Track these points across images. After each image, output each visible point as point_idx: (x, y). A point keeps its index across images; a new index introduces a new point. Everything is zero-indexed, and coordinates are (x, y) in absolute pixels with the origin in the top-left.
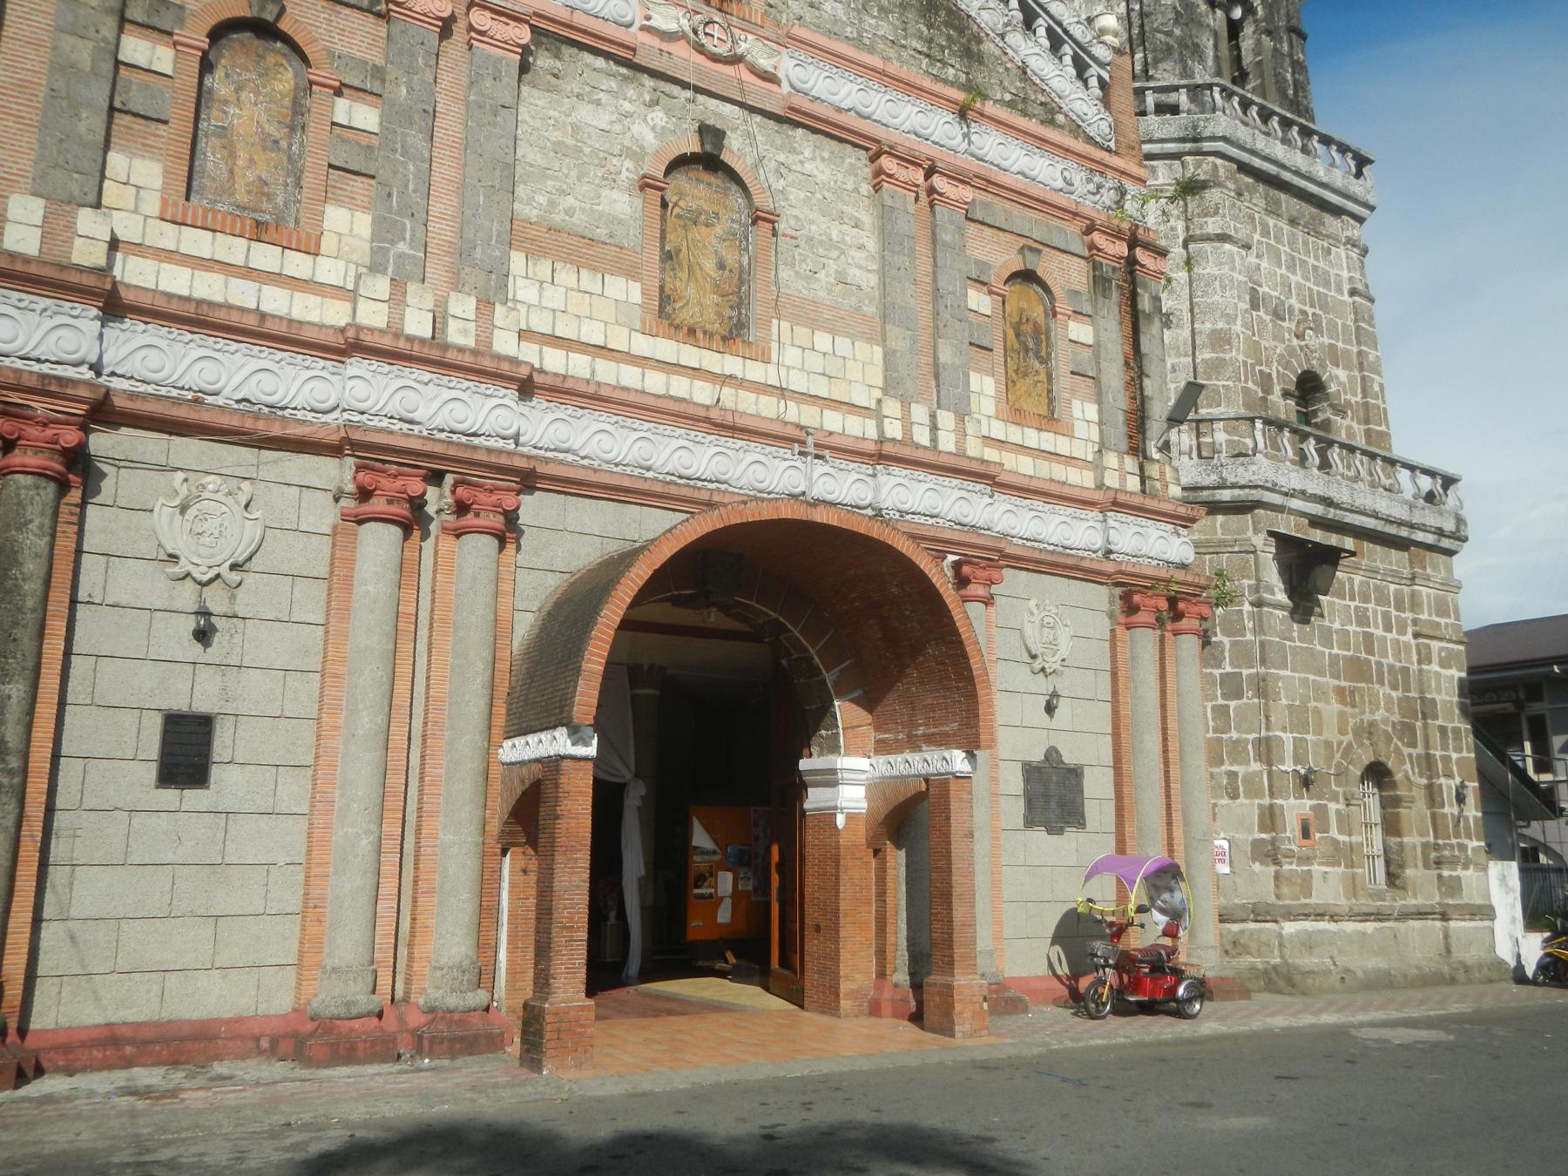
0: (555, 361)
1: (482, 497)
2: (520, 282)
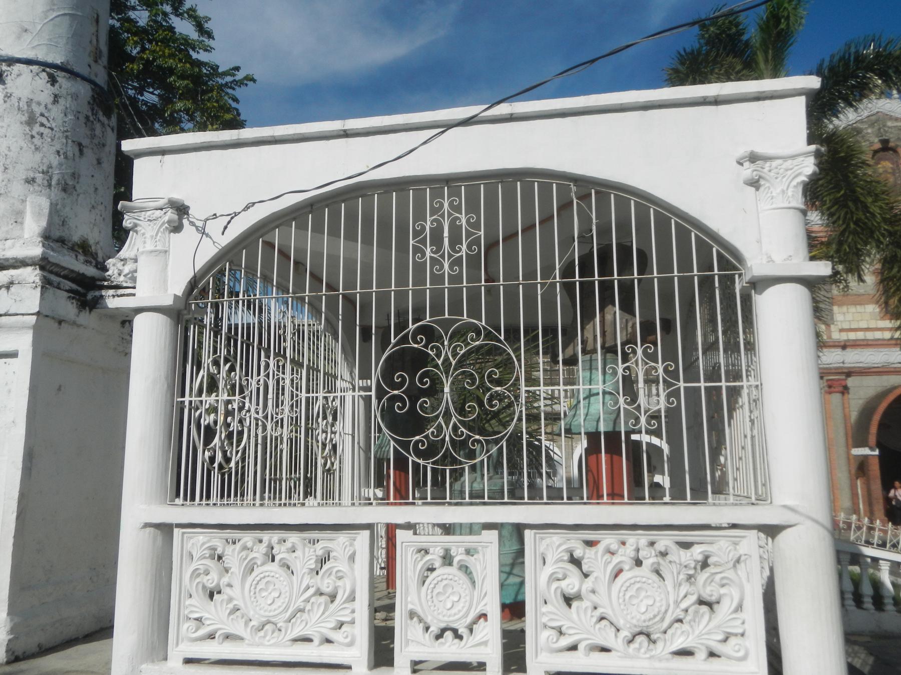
0: (852, 336)
2: (837, 315)
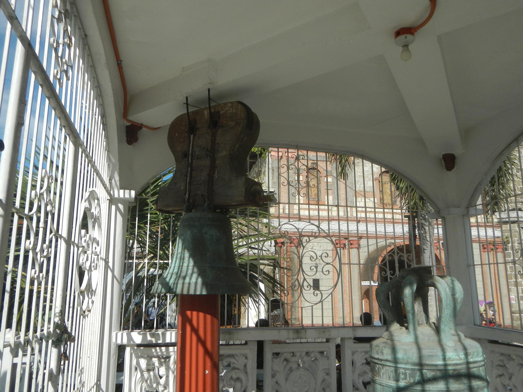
1: (355, 242)
